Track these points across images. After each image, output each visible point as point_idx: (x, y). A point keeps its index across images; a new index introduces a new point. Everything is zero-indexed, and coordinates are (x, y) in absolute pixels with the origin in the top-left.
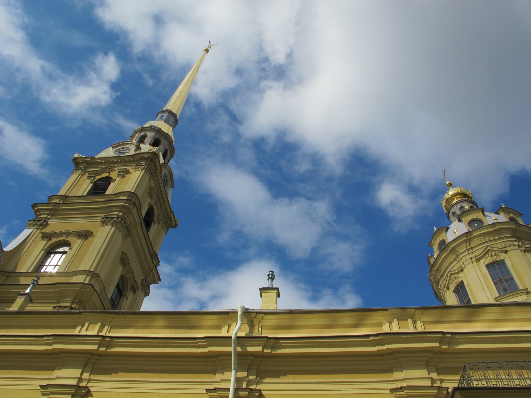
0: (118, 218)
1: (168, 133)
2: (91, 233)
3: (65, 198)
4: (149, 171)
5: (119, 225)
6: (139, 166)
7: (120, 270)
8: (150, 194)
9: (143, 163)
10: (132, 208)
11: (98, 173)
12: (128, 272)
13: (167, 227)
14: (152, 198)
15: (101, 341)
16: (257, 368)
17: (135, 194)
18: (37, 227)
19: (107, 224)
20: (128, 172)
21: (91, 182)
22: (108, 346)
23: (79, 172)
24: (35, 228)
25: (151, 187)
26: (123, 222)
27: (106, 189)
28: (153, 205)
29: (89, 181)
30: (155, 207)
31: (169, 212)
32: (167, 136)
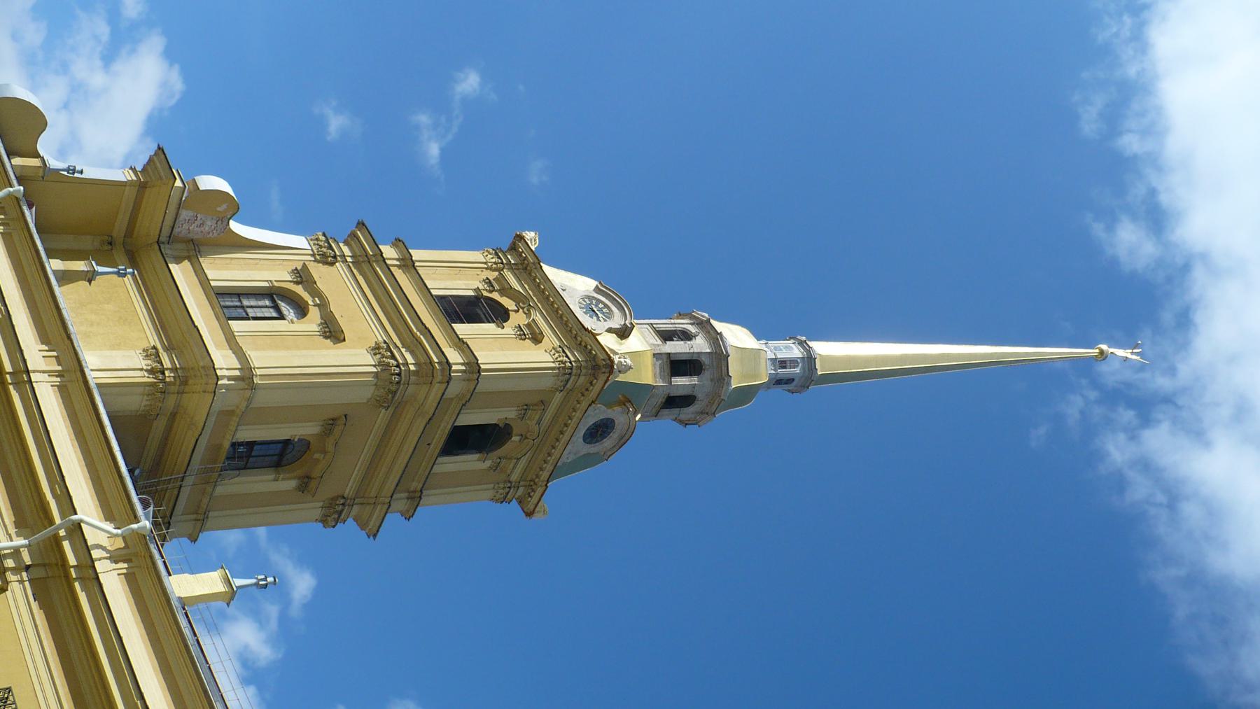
0: (398, 366)
1: (731, 377)
2: (342, 338)
3: (410, 263)
5: (386, 375)
6: (564, 352)
7: (305, 430)
9: (574, 356)
10: (438, 380)
11: (506, 290)
12: (325, 452)
15: (20, 372)
17: (479, 372)
18: (315, 251)
19: (375, 354)
20: (537, 338)
23: (492, 258)
24: (312, 250)
26: (396, 379)
30: (515, 438)
31: (542, 478)
32: (724, 380)
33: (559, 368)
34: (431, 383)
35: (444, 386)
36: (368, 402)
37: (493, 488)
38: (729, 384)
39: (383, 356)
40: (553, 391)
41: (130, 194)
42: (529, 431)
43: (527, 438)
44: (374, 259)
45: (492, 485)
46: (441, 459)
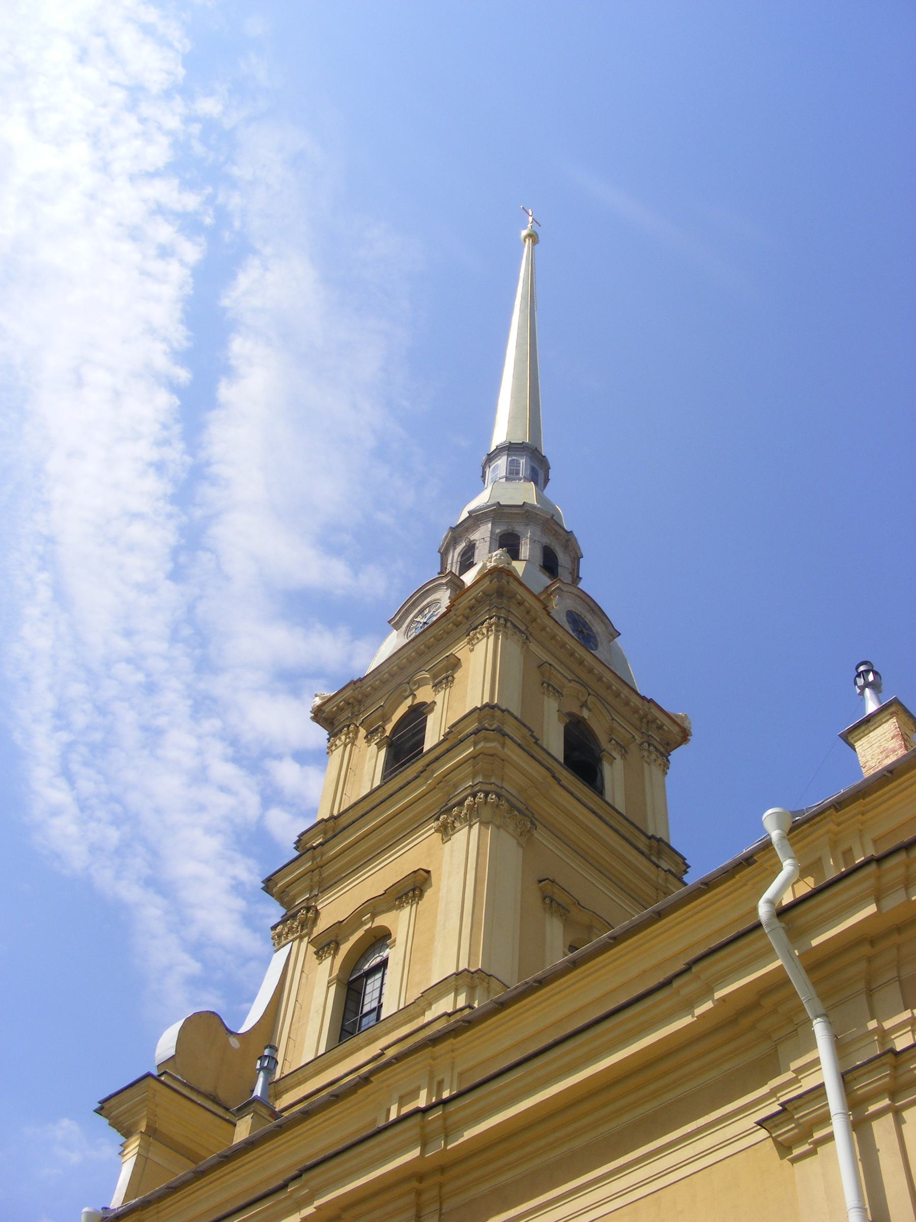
0: (474, 796)
2: (425, 874)
4: (509, 624)
8: (549, 685)
13: (657, 750)
14: (558, 693)
16: (899, 977)
18: (296, 935)
21: (379, 746)
22: (448, 1132)
23: (340, 739)
24: (293, 940)
25: (539, 667)
27: (422, 742)
28: (575, 710)
29: (374, 747)
30: (585, 714)
31: (641, 706)
32: (527, 511)
33: (497, 631)
34: (503, 760)
35: (508, 741)
36: (523, 847)
37: (649, 764)
38: (533, 506)
39: (458, 817)
40: (527, 652)
41: (160, 1155)
42: (578, 699)
43: (589, 695)
44: (318, 860)
45: (646, 765)
46: (608, 797)
